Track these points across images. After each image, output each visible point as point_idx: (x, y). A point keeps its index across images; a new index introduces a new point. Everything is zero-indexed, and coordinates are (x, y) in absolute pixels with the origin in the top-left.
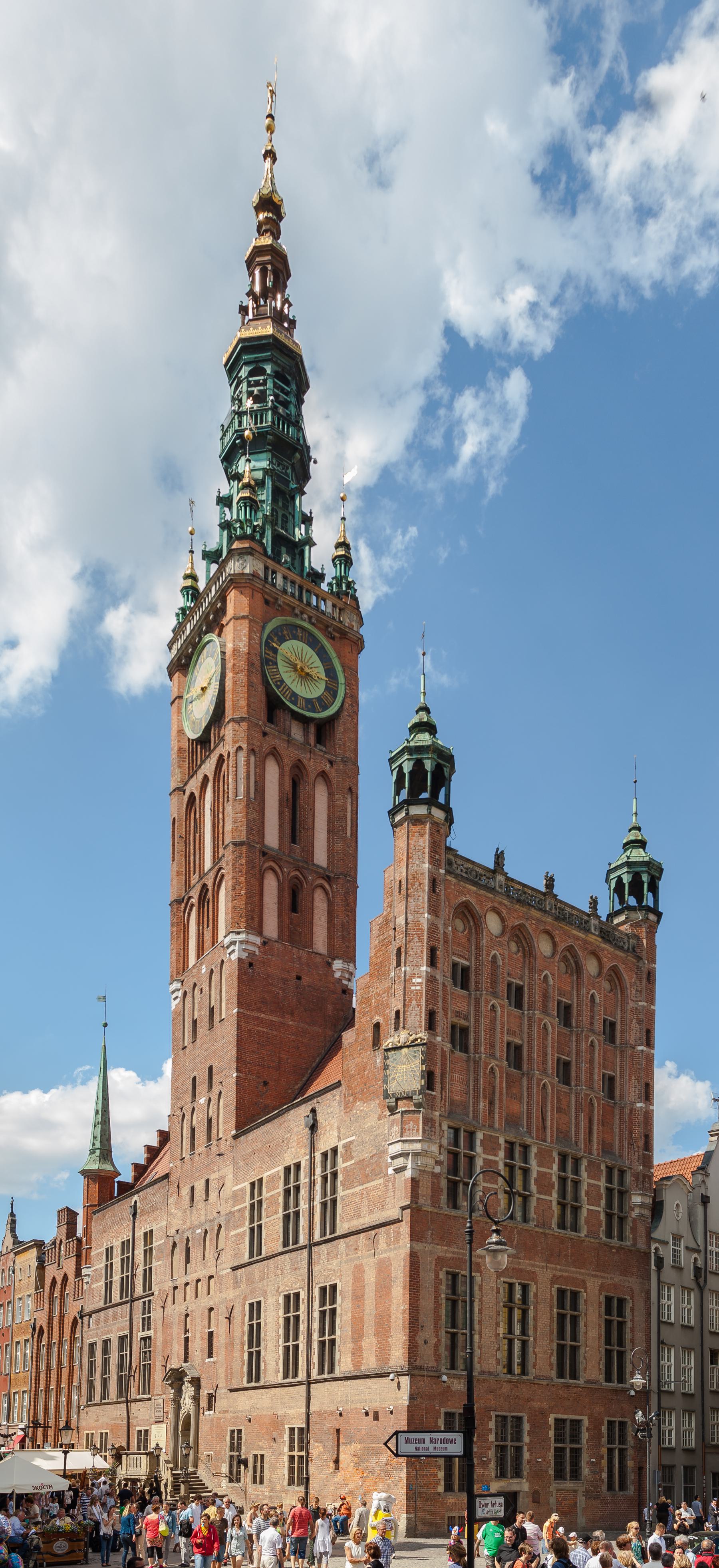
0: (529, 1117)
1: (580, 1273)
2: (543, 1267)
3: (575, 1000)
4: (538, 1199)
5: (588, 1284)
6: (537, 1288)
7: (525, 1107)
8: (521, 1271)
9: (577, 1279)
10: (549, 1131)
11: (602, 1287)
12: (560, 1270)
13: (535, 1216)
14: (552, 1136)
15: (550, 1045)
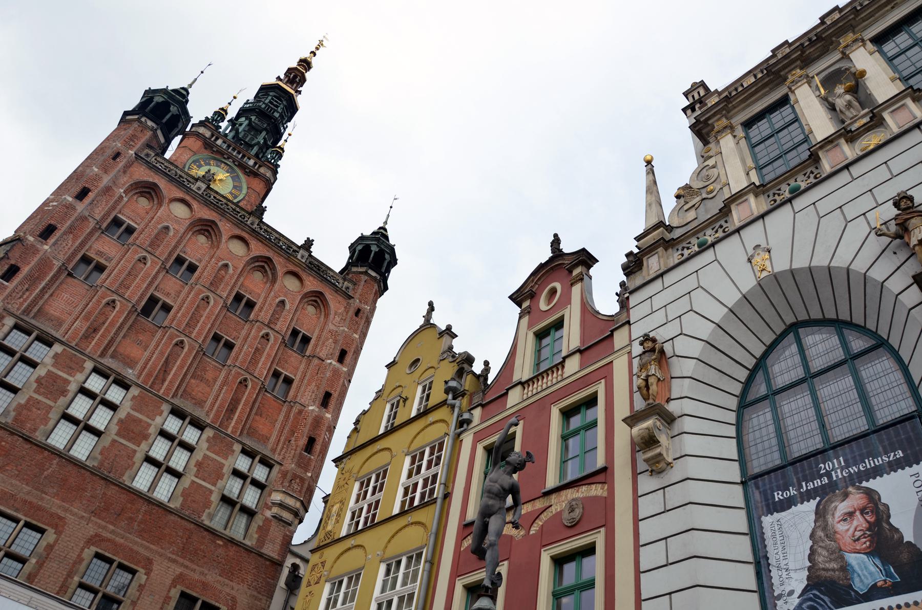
0: (146, 364)
1: (147, 548)
2: (82, 517)
3: (261, 300)
4: (114, 441)
5: (155, 567)
6: (56, 541)
7: (147, 354)
8: (39, 508)
9: (137, 553)
10: (166, 383)
11: (179, 579)
12: (112, 532)
13: (99, 457)
14: (168, 389)
15: (205, 314)
